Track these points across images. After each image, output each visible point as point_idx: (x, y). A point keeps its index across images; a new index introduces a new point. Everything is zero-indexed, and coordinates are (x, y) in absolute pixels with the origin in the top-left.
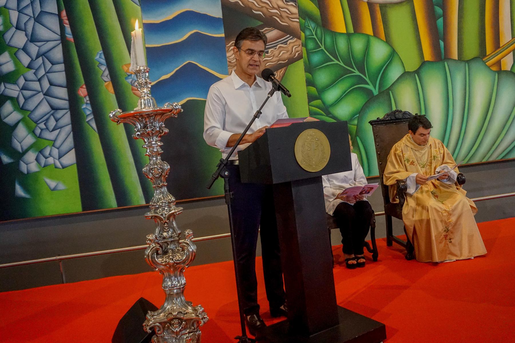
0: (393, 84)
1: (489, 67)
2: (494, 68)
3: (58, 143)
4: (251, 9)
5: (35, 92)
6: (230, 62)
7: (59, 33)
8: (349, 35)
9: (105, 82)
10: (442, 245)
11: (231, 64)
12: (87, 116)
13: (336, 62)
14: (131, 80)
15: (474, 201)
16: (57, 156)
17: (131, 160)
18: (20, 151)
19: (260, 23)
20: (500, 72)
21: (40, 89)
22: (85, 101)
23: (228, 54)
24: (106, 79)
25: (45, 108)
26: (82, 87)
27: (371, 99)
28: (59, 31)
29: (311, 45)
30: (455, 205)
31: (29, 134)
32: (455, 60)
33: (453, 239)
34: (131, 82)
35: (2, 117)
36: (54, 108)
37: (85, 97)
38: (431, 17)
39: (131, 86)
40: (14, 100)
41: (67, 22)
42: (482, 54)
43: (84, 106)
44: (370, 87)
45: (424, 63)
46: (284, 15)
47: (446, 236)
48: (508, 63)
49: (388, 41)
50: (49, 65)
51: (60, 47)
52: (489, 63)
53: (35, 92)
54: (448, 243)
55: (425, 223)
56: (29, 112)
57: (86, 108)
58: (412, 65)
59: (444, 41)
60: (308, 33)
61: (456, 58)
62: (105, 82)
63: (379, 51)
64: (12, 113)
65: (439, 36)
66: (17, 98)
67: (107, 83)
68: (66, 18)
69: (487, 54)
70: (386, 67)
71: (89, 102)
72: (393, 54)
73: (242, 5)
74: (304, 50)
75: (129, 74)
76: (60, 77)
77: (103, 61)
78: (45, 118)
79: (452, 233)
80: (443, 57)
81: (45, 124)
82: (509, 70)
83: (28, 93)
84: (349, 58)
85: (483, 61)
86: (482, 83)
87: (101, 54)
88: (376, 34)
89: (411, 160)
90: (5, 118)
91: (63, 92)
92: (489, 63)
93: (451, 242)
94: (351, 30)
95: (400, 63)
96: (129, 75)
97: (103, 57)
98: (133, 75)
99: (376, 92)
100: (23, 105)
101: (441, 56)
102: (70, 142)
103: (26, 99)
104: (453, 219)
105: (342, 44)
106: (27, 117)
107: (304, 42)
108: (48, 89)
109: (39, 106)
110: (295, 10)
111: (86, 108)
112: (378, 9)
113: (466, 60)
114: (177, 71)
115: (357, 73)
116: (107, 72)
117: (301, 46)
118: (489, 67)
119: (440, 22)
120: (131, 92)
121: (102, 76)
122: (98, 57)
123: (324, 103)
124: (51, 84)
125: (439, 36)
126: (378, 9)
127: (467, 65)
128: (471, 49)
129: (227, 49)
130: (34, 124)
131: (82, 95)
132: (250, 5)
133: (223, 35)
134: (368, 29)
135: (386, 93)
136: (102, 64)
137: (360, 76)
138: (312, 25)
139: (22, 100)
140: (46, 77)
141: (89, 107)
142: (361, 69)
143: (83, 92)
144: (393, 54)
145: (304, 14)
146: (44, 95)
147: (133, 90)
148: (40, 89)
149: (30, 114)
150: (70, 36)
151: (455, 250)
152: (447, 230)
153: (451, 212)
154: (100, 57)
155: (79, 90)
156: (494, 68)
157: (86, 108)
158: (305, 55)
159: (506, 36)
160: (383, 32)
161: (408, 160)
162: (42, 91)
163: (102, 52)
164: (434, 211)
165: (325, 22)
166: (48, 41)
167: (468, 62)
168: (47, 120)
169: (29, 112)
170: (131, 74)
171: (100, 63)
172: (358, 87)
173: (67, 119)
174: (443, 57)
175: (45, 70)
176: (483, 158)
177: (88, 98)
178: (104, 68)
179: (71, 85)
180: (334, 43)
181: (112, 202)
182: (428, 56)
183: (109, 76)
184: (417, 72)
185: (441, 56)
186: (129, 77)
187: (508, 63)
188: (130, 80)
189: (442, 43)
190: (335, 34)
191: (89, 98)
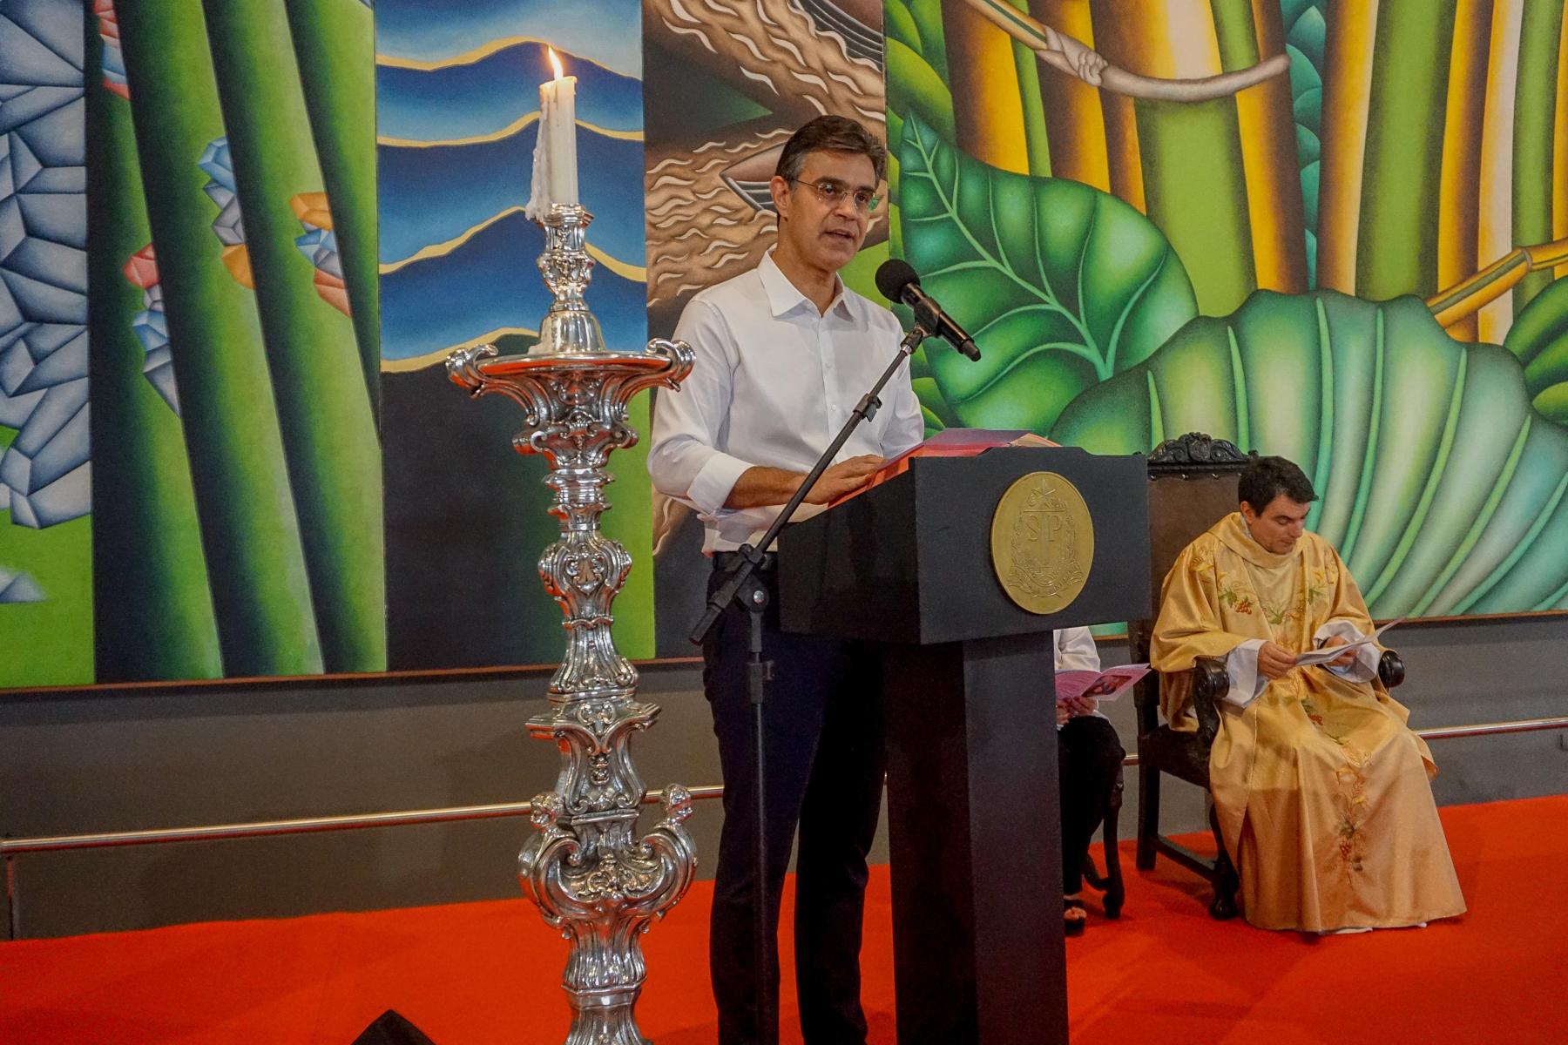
0: (1159, 352)
1: (1443, 329)
2: (1458, 334)
3: (32, 439)
4: (737, 64)
6: (654, 225)
7: (81, 66)
8: (1035, 183)
9: (227, 245)
10: (1333, 877)
11: (657, 233)
12: (151, 353)
13: (991, 262)
14: (315, 248)
15: (1425, 738)
16: (24, 485)
17: (289, 517)
19: (761, 112)
20: (1473, 346)
22: (148, 301)
23: (650, 201)
24: (228, 235)
26: (141, 255)
27: (1089, 392)
28: (79, 55)
29: (916, 201)
30: (1378, 749)
32: (1348, 296)
33: (1366, 858)
34: (316, 256)
36: (33, 317)
37: (149, 288)
38: (1286, 158)
39: (313, 269)
41: (113, 27)
42: (1425, 290)
43: (142, 320)
44: (1090, 352)
45: (1254, 296)
46: (841, 94)
47: (1346, 849)
48: (1497, 322)
49: (1153, 216)
50: (30, 166)
51: (78, 111)
52: (1443, 316)
54: (1351, 871)
55: (1283, 801)
57: (150, 327)
58: (1221, 299)
59: (1319, 233)
60: (910, 161)
61: (1350, 288)
62: (227, 245)
63: (1124, 246)
65: (1303, 218)
67: (230, 250)
68: (110, 14)
69: (1440, 289)
70: (1144, 295)
71: (159, 307)
72: (1165, 258)
73: (710, 47)
74: (894, 212)
75: (313, 227)
76: (67, 212)
77: (227, 175)
79: (1363, 838)
80: (1312, 283)
82: (1501, 343)
84: (1032, 258)
85: (1428, 310)
86: (1419, 374)
87: (219, 148)
88: (1118, 190)
89: (1241, 597)
91: (71, 265)
92: (1443, 316)
93: (1359, 869)
94: (1045, 170)
95: (1184, 288)
96: (310, 233)
97: (227, 158)
98: (324, 234)
99: (1105, 372)
101: (1306, 279)
102: (77, 438)
104: (1371, 795)
105: (1013, 208)
107: (896, 191)
110: (875, 85)
112: (1130, 112)
113: (1382, 297)
114: (476, 237)
115: (1054, 305)
116: (235, 213)
117: (885, 199)
118: (1443, 329)
119: (1311, 172)
120: (312, 285)
121: (217, 223)
122: (209, 158)
123: (942, 387)
124: (32, 231)
125: (1303, 218)
126: (1130, 112)
127: (1380, 313)
128: (1396, 272)
129: (647, 182)
131: (138, 279)
132: (737, 51)
133: (639, 136)
134: (1097, 172)
135: (1137, 379)
136: (221, 185)
137: (1060, 314)
138: (925, 138)
140: (14, 205)
141: (161, 326)
142: (1068, 298)
143: (142, 269)
144: (1165, 258)
145: (902, 99)
147: (318, 281)
150: (116, 77)
151: (1370, 895)
152: (1349, 831)
153: (1364, 774)
154: (216, 160)
155: (128, 263)
156: (1458, 334)
157: (150, 327)
158: (895, 230)
159: (1496, 244)
160: (1140, 184)
161: (1232, 597)
163: (225, 142)
164: (1314, 762)
165: (965, 135)
166: (36, 84)
167: (1384, 305)
170: (318, 231)
171: (214, 180)
172: (1051, 351)
173: (73, 356)
174: (1312, 283)
175: (15, 177)
176: (1412, 607)
177: (157, 294)
178: (225, 197)
179: (102, 242)
180: (990, 203)
181: (209, 661)
182: (1268, 275)
183: (240, 228)
184: (1234, 320)
185: (1306, 279)
186: (312, 239)
187: (1497, 322)
188: (312, 249)
189: (1311, 241)
190: (993, 176)
191: (165, 292)
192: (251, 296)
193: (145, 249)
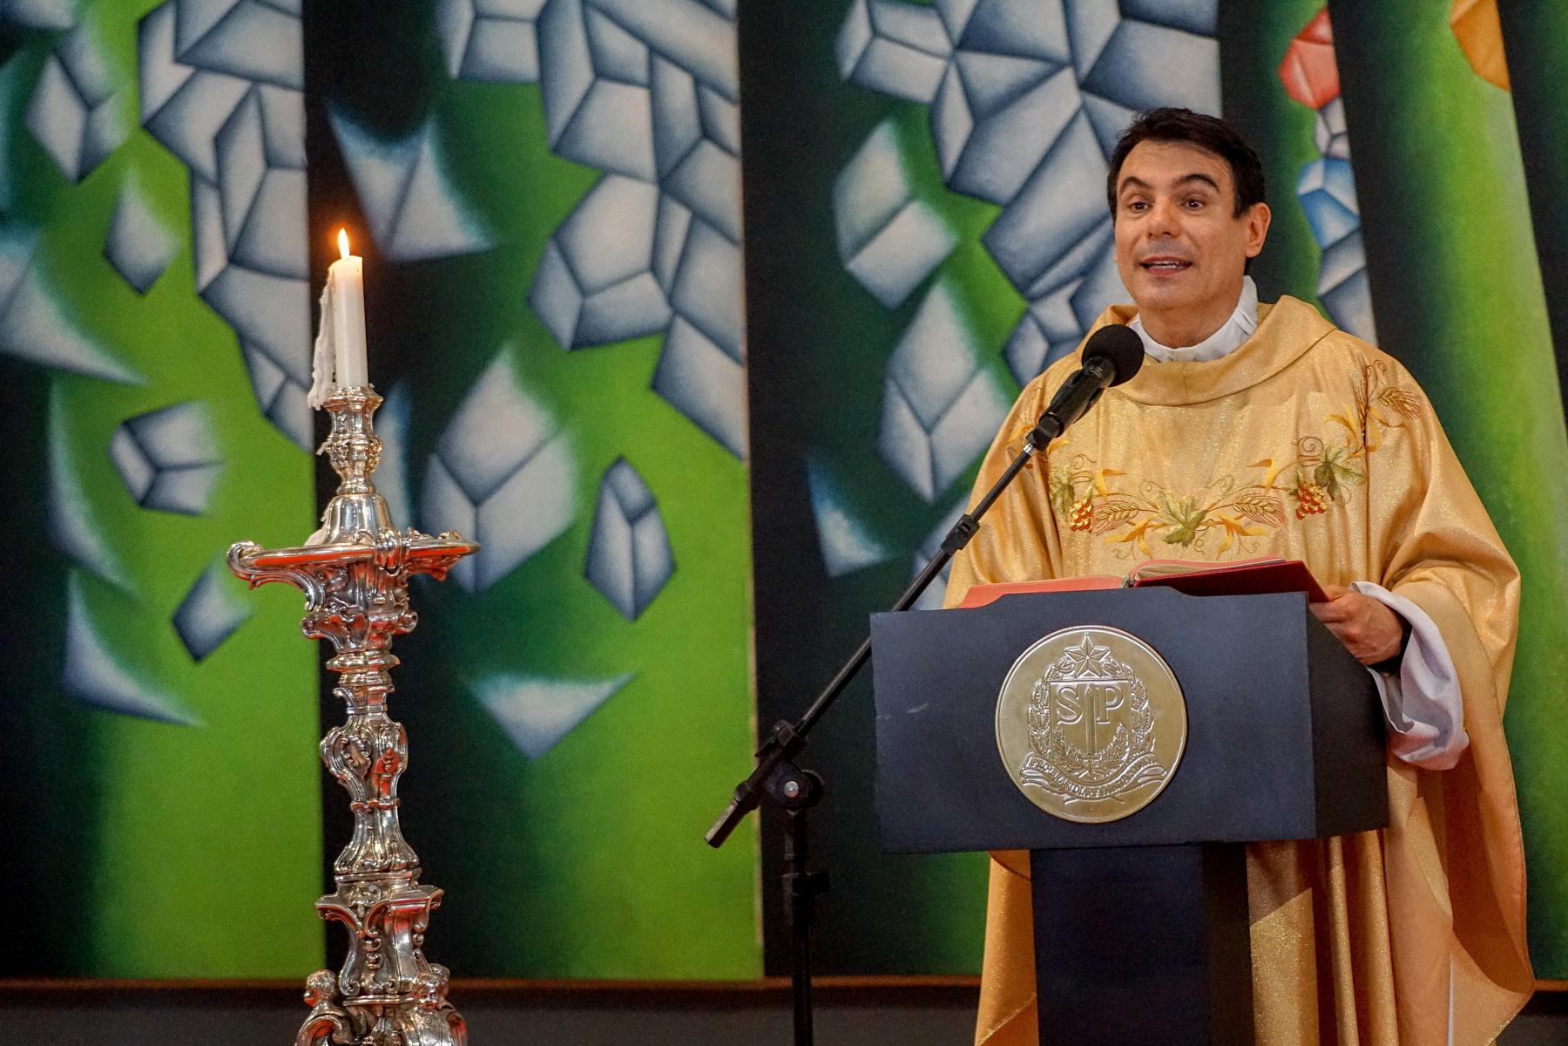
5: (1027, 68)
12: (1329, 252)
18: (924, 484)
21: (1059, 47)
22: (1323, 136)
25: (1077, 186)
26: (1307, 36)
31: (980, 366)
35: (846, 240)
37: (1323, 108)
40: (916, 120)
43: (1312, 181)
53: (1027, 68)
56: (991, 213)
64: (894, 213)
66: (933, 110)
71: (1342, 148)
78: (1079, 256)
81: (1073, 302)
83: (993, 72)
90: (862, 242)
100: (962, 159)
103: (984, 114)
106: (979, 252)
108: (1112, 46)
109: (1049, 175)
111: (1321, 193)
130: (1012, 301)
139: (956, 125)
141: (1343, 189)
146: (1087, 85)
148: (1059, 47)
149: (996, 225)
155: (1287, 52)
162: (1074, 62)
168: (1089, 272)
169: (991, 213)
192: (1502, 103)
193: (1314, 23)
